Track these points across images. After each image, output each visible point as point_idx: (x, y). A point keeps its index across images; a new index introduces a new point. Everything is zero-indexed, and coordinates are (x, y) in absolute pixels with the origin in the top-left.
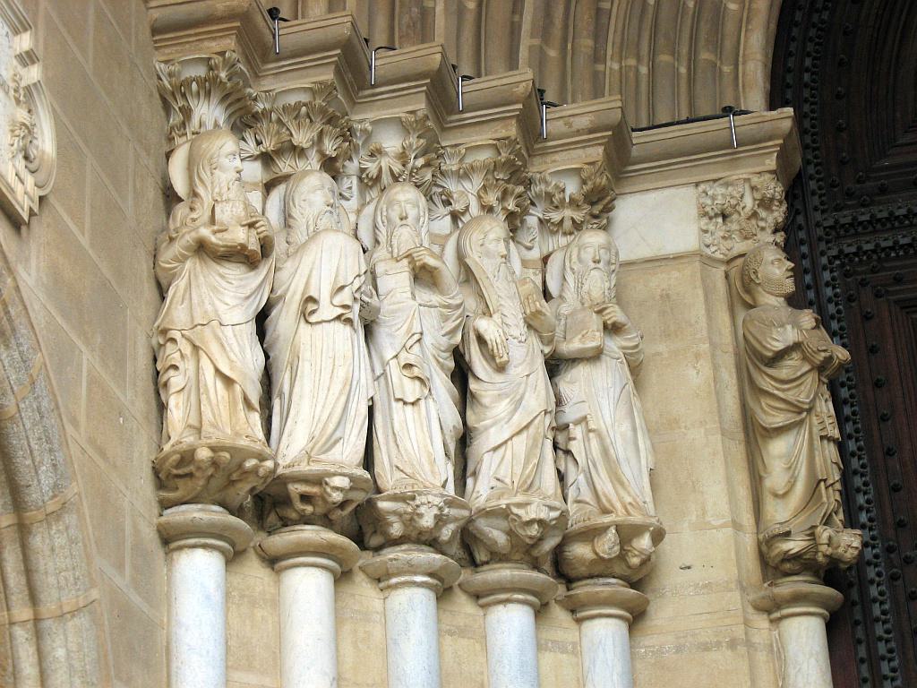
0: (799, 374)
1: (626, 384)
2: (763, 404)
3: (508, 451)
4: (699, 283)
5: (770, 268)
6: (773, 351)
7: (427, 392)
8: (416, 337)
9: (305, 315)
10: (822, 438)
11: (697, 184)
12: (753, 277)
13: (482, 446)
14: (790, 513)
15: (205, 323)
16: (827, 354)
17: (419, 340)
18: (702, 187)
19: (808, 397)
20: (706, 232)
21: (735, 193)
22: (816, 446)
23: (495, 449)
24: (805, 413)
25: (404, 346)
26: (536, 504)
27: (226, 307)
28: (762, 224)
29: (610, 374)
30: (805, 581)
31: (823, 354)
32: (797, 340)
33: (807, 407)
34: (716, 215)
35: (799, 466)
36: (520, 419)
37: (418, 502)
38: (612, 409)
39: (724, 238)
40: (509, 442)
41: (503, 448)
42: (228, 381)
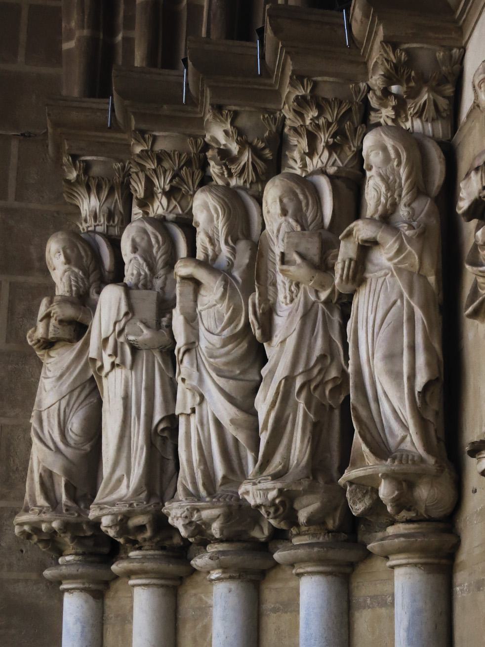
1: (395, 303)
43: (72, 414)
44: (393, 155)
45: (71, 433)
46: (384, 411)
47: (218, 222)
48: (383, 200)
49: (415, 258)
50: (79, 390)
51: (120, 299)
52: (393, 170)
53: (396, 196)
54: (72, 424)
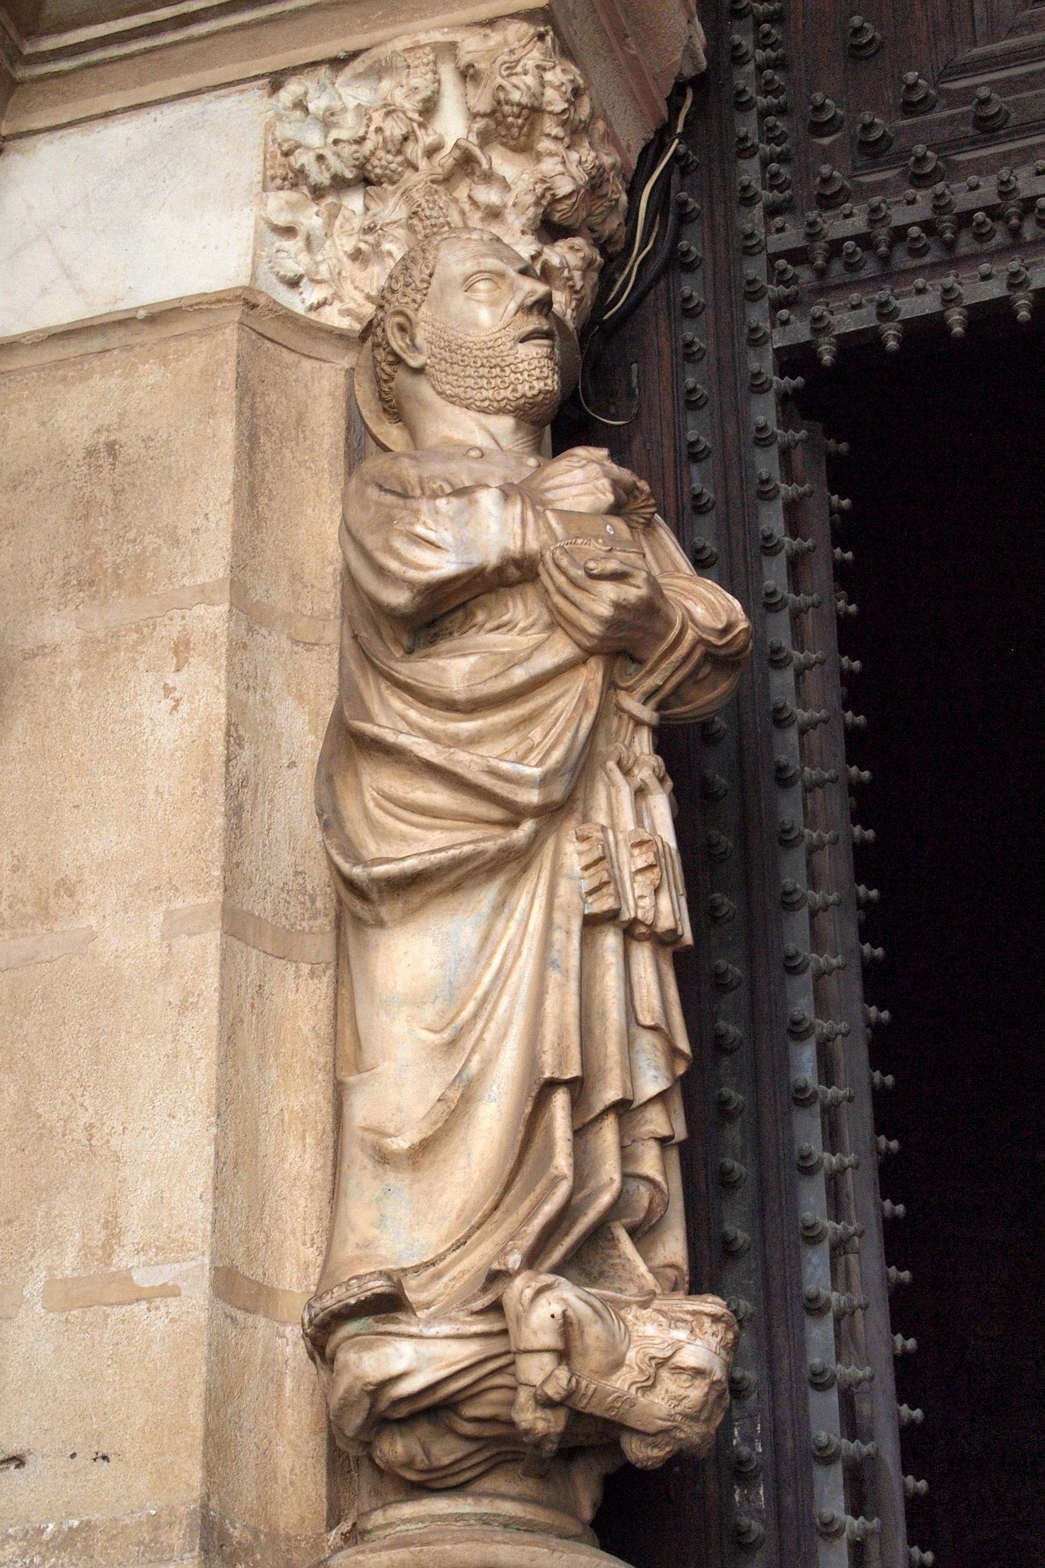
0: (519, 675)
2: (369, 794)
4: (226, 398)
5: (458, 301)
6: (411, 584)
10: (592, 923)
11: (276, 81)
12: (397, 343)
14: (444, 1231)
16: (633, 592)
18: (293, 89)
19: (539, 764)
20: (289, 231)
21: (399, 98)
22: (555, 955)
24: (527, 827)
28: (488, 195)
30: (509, 1524)
31: (610, 591)
32: (514, 546)
33: (532, 797)
34: (340, 184)
35: (488, 1036)
39: (357, 255)
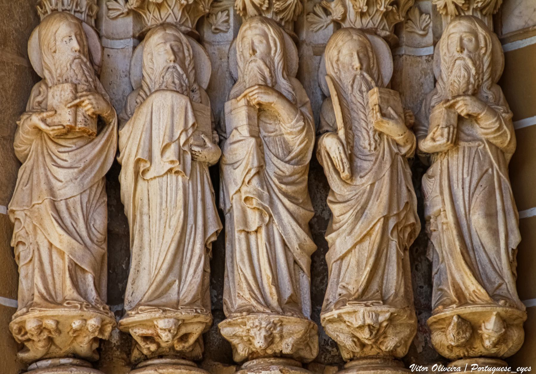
1: (487, 171)
3: (352, 259)
7: (267, 219)
8: (253, 172)
9: (137, 174)
13: (331, 257)
15: (40, 202)
17: (258, 173)
23: (342, 258)
25: (243, 181)
26: (362, 311)
27: (60, 184)
29: (466, 164)
36: (360, 229)
37: (248, 327)
38: (467, 199)
40: (353, 251)
41: (350, 256)
42: (61, 253)
43: (92, 209)
44: (482, 44)
45: (93, 229)
46: (479, 260)
47: (275, 56)
48: (472, 80)
49: (507, 137)
50: (96, 186)
51: (186, 108)
52: (479, 55)
53: (480, 79)
54: (95, 220)
